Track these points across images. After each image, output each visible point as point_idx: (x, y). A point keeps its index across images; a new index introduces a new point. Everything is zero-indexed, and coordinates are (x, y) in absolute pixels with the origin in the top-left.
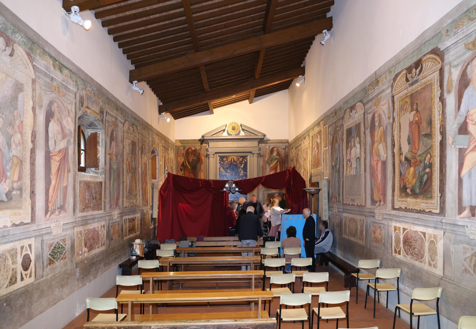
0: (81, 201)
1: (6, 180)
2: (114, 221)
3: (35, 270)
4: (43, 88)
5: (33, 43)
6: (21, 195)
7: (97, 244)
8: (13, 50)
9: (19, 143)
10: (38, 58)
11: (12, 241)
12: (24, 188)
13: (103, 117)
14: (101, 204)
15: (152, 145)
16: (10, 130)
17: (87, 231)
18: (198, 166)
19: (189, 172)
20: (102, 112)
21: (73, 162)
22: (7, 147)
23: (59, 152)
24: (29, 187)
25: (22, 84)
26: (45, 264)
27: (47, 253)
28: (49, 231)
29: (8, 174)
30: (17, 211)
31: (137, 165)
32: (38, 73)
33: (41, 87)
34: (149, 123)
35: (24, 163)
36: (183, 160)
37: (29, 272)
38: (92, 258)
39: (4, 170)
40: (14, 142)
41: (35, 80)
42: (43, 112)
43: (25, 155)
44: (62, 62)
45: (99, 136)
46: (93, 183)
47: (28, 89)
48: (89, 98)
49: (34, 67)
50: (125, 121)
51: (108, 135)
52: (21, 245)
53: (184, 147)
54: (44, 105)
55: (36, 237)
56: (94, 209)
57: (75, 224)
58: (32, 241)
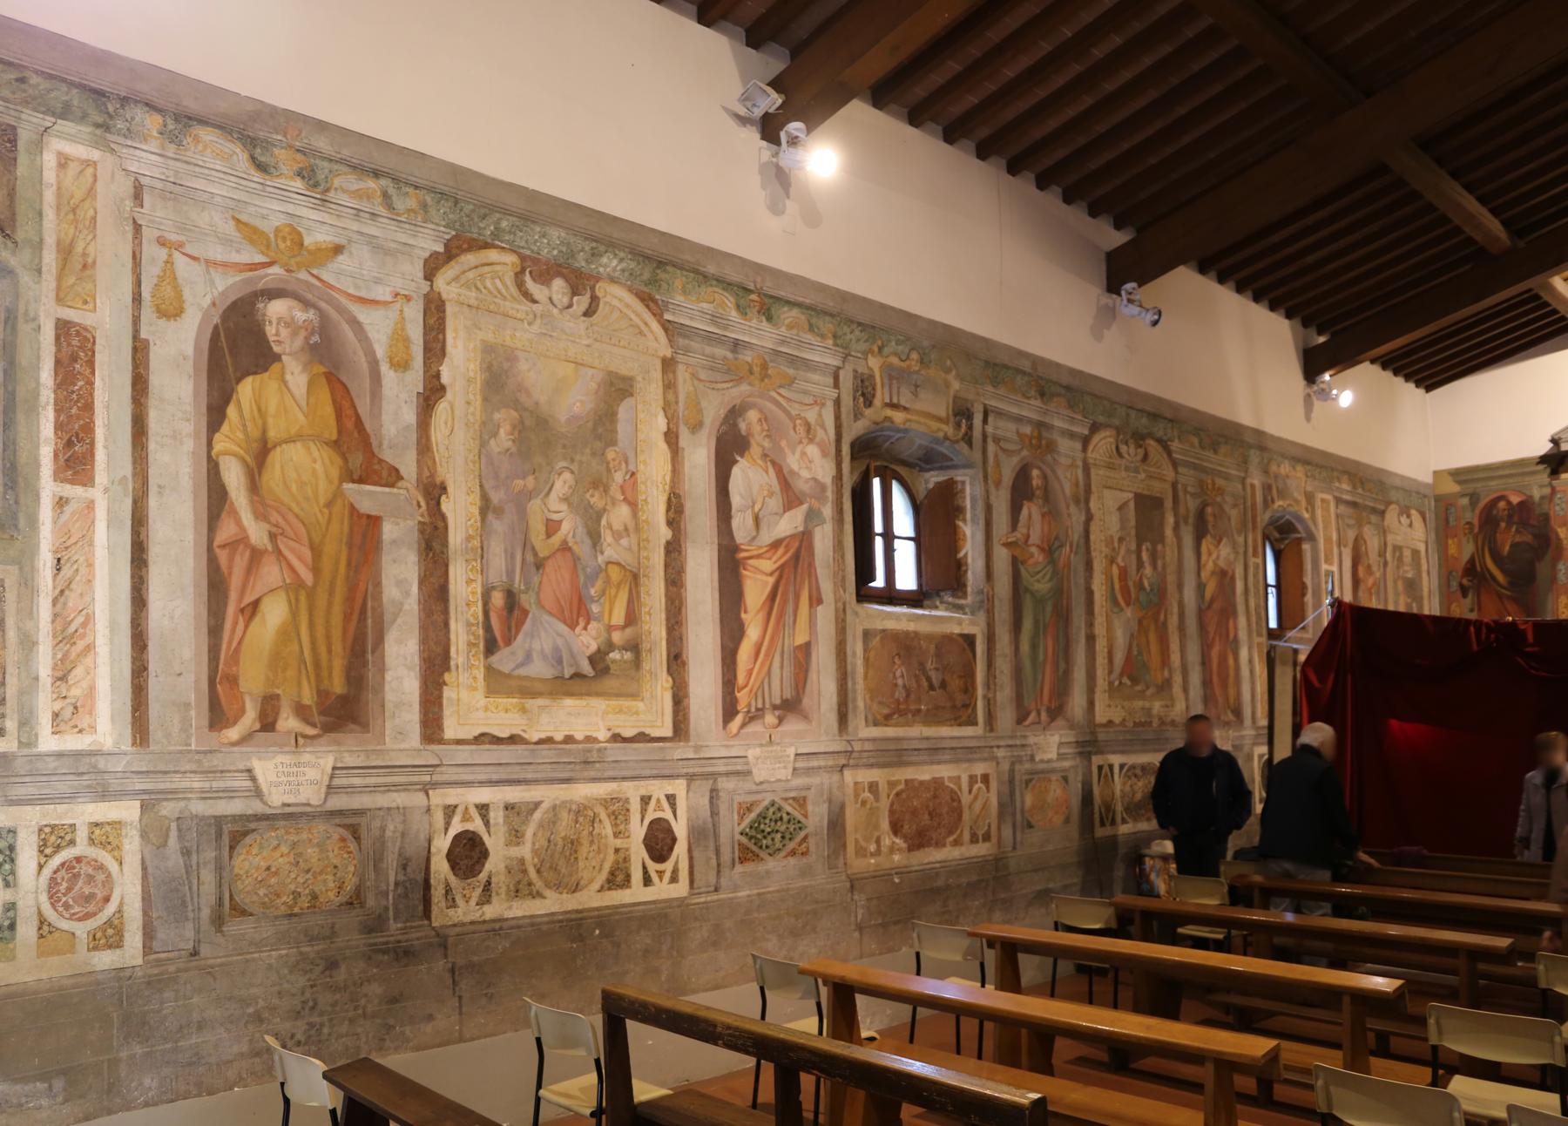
0: (873, 693)
1: (588, 623)
2: (1042, 766)
3: (691, 867)
4: (702, 377)
5: (661, 264)
6: (637, 663)
7: (951, 833)
8: (594, 299)
9: (626, 529)
10: (679, 299)
11: (614, 779)
12: (645, 646)
13: (970, 427)
14: (969, 705)
15: (1267, 503)
16: (596, 500)
17: (902, 787)
18: (1542, 568)
19: (1500, 596)
20: (962, 413)
21: (835, 575)
22: (588, 541)
23: (775, 545)
24: (664, 643)
25: (629, 380)
26: (726, 856)
27: (731, 827)
28: (739, 768)
29: (595, 608)
30: (626, 703)
31: (1171, 579)
32: (681, 341)
33: (694, 376)
34: (1246, 418)
35: (643, 580)
36: (1468, 549)
37: (668, 866)
38: (929, 874)
39: (580, 599)
40: (610, 527)
41: (672, 359)
42: (704, 441)
43: (648, 558)
44: (772, 292)
45: (963, 491)
46: (930, 637)
47: (651, 391)
48: (895, 376)
49: (667, 326)
50: (1095, 428)
51: (998, 484)
52: (643, 792)
53: (1474, 498)
54: (708, 421)
55: (691, 778)
56: (933, 718)
57: (847, 759)
58: (678, 787)
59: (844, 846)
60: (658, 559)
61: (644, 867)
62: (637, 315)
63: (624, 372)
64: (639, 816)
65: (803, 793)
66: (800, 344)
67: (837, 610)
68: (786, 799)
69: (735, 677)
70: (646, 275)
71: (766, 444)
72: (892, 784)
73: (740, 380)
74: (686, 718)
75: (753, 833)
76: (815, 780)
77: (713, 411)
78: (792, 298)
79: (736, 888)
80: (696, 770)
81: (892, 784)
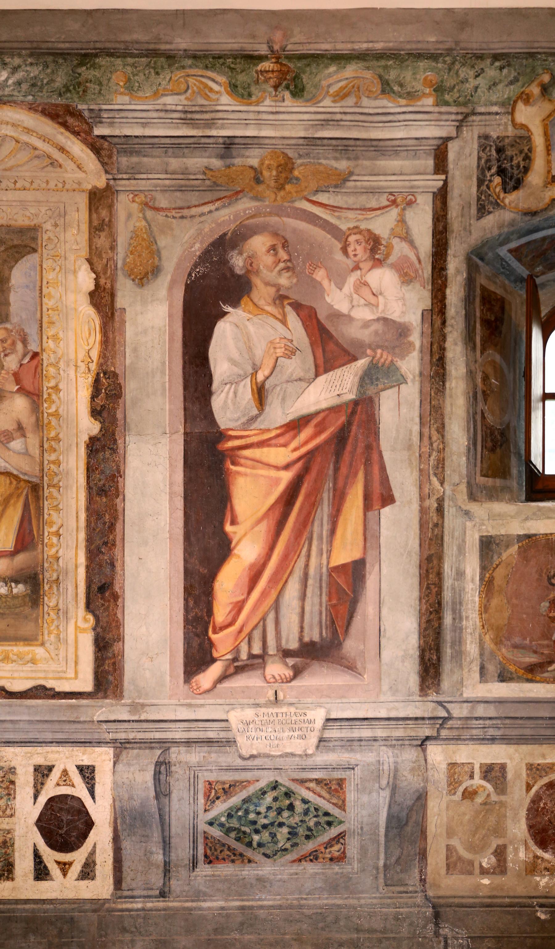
5: (86, 58)
6: (35, 597)
9: (20, 428)
10: (121, 101)
12: (49, 575)
23: (296, 425)
24: (82, 573)
26: (182, 851)
27: (188, 811)
32: (124, 161)
37: (78, 857)
41: (108, 187)
42: (163, 292)
43: (58, 463)
49: (97, 146)
52: (40, 761)
55: (121, 747)
59: (423, 855)
60: (74, 465)
61: (37, 856)
62: (44, 139)
63: (21, 221)
64: (31, 791)
65: (338, 775)
68: (302, 782)
70: (60, 80)
72: (535, 771)
75: (234, 823)
76: (364, 758)
77: (180, 246)
78: (343, 48)
79: (198, 896)
80: (131, 736)
81: (535, 771)
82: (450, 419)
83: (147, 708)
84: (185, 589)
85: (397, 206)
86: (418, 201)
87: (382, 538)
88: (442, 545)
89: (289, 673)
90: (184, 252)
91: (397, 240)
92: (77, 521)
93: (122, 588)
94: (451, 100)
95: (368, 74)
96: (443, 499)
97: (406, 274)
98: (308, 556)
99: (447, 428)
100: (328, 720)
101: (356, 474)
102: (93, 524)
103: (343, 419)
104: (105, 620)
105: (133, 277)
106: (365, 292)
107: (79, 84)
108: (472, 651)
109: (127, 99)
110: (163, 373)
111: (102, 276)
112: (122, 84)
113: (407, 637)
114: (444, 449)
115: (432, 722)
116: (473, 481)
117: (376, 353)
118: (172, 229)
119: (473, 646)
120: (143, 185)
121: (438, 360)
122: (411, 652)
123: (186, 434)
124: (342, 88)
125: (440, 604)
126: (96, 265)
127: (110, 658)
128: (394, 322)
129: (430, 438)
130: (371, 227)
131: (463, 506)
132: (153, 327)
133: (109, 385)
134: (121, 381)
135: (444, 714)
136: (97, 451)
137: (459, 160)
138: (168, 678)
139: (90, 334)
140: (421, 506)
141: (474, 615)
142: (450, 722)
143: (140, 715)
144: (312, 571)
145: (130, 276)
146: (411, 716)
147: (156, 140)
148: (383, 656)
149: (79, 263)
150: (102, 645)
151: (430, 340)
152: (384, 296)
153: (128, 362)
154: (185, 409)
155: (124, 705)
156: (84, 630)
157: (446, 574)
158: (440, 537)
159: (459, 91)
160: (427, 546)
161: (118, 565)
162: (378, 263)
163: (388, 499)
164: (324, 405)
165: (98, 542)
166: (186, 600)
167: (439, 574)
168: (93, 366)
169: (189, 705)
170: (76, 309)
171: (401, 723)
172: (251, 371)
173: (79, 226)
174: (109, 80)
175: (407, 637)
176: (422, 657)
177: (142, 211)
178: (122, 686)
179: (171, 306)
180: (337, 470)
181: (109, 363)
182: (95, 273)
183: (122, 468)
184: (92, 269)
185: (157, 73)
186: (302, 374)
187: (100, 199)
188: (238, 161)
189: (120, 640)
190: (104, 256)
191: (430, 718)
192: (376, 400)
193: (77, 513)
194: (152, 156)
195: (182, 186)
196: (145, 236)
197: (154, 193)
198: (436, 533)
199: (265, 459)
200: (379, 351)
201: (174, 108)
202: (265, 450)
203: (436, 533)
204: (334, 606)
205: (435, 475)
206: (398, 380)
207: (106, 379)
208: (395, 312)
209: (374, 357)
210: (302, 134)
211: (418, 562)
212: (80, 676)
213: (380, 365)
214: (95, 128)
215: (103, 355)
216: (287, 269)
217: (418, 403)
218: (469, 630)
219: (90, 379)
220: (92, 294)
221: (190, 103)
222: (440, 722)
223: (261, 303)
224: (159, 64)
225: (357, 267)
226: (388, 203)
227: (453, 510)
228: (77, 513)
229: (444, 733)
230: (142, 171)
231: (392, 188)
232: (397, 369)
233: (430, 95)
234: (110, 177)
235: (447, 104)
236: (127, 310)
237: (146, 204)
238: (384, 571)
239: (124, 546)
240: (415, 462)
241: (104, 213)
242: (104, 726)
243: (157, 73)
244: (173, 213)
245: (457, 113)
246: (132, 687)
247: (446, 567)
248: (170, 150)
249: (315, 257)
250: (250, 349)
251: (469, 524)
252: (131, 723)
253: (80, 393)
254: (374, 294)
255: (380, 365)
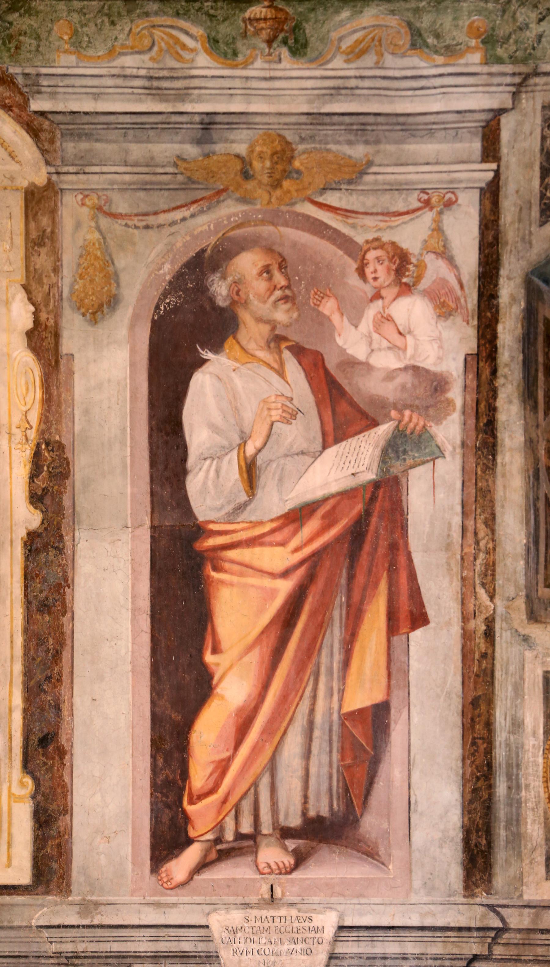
10: (66, 62)
23: (297, 516)
28: (186, 947)
32: (71, 147)
41: (50, 184)
42: (123, 332)
66: (389, 84)
67: (467, 636)
69: (185, 775)
71: (281, 315)
73: (219, 194)
74: (63, 851)
77: (145, 268)
80: (81, 947)
82: (503, 507)
83: (102, 908)
84: (153, 742)
85: (431, 209)
86: (460, 201)
87: (411, 673)
88: (492, 683)
89: (289, 860)
90: (150, 275)
91: (432, 256)
92: (12, 648)
93: (70, 740)
94: (505, 56)
95: (393, 21)
96: (493, 620)
97: (443, 304)
98: (314, 698)
99: (498, 520)
100: (341, 928)
101: (376, 585)
102: (32, 652)
103: (359, 507)
104: (47, 784)
105: (83, 310)
106: (388, 329)
107: (11, 37)
108: (535, 834)
109: (72, 59)
110: (123, 443)
111: (43, 309)
112: (66, 37)
113: (447, 812)
114: (494, 549)
115: (481, 934)
116: (534, 595)
117: (403, 416)
118: (134, 244)
119: (536, 827)
120: (95, 181)
121: (486, 425)
122: (452, 833)
123: (153, 528)
124: (358, 42)
125: (490, 765)
126: (35, 293)
127: (54, 838)
128: (427, 371)
129: (476, 534)
130: (395, 239)
131: (520, 630)
132: (109, 381)
133: (53, 461)
134: (68, 455)
135: (497, 923)
136: (37, 551)
137: (515, 141)
138: (130, 866)
139: (27, 389)
140: (463, 629)
141: (537, 783)
142: (506, 936)
143: (93, 917)
144: (319, 718)
145: (79, 309)
146: (452, 925)
147: (112, 118)
148: (413, 839)
149: (12, 290)
150: (43, 819)
151: (475, 396)
152: (414, 336)
153: (77, 428)
154: (152, 494)
155: (72, 904)
156: (19, 799)
157: (497, 724)
158: (489, 672)
159: (516, 42)
160: (472, 685)
161: (65, 708)
162: (406, 289)
163: (419, 619)
164: (334, 488)
165: (39, 676)
166: (153, 757)
167: (489, 725)
168: (32, 435)
169: (157, 905)
170: (9, 355)
171: (439, 934)
172: (238, 441)
173: (12, 239)
174: (50, 32)
175: (447, 812)
176: (466, 841)
177: (94, 218)
178: (70, 876)
179: (133, 351)
180: (351, 578)
181: (53, 430)
182: (33, 304)
183: (70, 575)
184: (30, 299)
185: (113, 23)
186: (304, 446)
187: (39, 201)
188: (219, 148)
189: (67, 812)
190: (45, 280)
191: (478, 929)
192: (404, 481)
193: (12, 636)
194: (108, 141)
195: (146, 183)
196: (99, 253)
197: (109, 193)
198: (484, 666)
199: (256, 563)
200: (407, 413)
201: (135, 72)
202: (257, 550)
203: (484, 666)
204: (348, 768)
205: (483, 585)
206: (433, 453)
207: (49, 451)
208: (429, 359)
209: (400, 422)
210: (305, 109)
211: (460, 707)
212: (15, 862)
213: (408, 432)
214: (31, 101)
215: (45, 419)
216: (285, 299)
217: (459, 485)
218: (530, 805)
219: (28, 453)
220: (30, 334)
221: (156, 66)
222: (492, 934)
223: (251, 346)
224: (115, 10)
225: (377, 296)
226: (420, 205)
227: (507, 635)
228: (12, 636)
229: (498, 951)
230: (94, 161)
231: (425, 183)
232: (432, 437)
233: (476, 48)
234: (52, 170)
235: (499, 61)
236: (76, 356)
237: (100, 209)
238: (415, 719)
239: (72, 682)
240: (456, 568)
241: (45, 221)
242: (46, 933)
243: (113, 23)
244: (135, 221)
245: (514, 74)
246: (82, 879)
247: (498, 714)
248: (131, 132)
249: (322, 283)
250: (236, 411)
251: (528, 654)
252: (81, 930)
253: (15, 471)
254: (400, 333)
255: (408, 432)
